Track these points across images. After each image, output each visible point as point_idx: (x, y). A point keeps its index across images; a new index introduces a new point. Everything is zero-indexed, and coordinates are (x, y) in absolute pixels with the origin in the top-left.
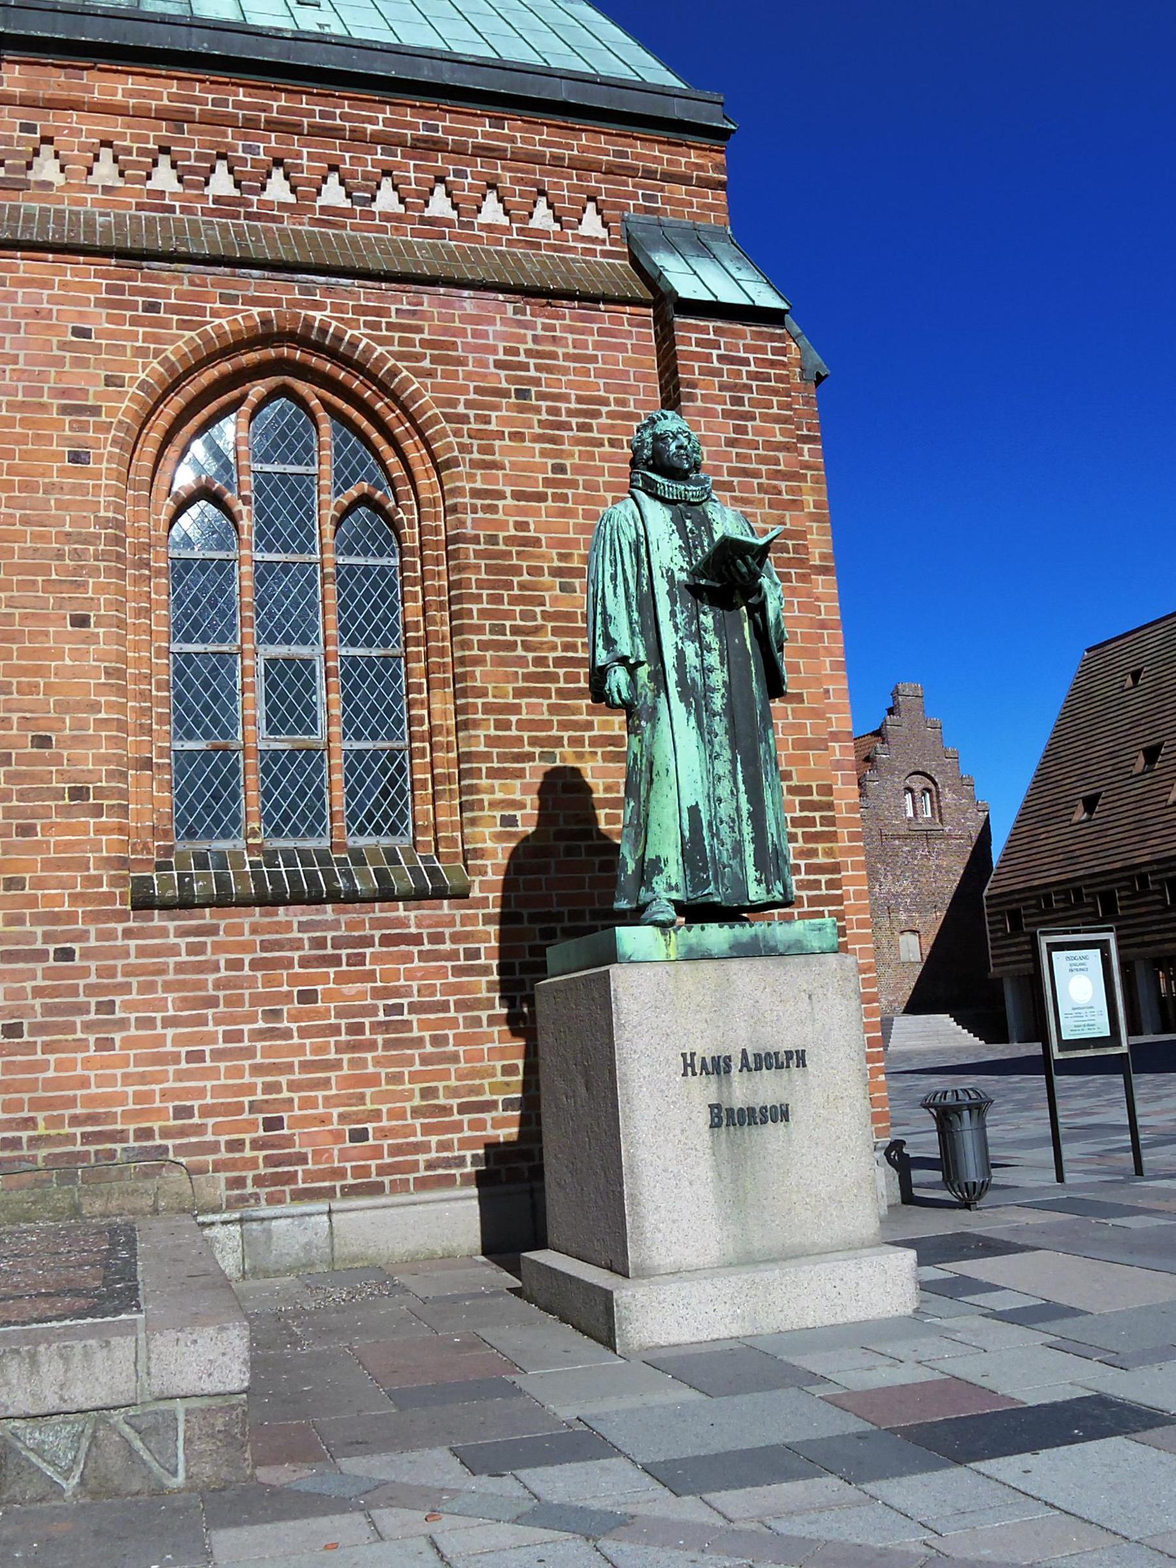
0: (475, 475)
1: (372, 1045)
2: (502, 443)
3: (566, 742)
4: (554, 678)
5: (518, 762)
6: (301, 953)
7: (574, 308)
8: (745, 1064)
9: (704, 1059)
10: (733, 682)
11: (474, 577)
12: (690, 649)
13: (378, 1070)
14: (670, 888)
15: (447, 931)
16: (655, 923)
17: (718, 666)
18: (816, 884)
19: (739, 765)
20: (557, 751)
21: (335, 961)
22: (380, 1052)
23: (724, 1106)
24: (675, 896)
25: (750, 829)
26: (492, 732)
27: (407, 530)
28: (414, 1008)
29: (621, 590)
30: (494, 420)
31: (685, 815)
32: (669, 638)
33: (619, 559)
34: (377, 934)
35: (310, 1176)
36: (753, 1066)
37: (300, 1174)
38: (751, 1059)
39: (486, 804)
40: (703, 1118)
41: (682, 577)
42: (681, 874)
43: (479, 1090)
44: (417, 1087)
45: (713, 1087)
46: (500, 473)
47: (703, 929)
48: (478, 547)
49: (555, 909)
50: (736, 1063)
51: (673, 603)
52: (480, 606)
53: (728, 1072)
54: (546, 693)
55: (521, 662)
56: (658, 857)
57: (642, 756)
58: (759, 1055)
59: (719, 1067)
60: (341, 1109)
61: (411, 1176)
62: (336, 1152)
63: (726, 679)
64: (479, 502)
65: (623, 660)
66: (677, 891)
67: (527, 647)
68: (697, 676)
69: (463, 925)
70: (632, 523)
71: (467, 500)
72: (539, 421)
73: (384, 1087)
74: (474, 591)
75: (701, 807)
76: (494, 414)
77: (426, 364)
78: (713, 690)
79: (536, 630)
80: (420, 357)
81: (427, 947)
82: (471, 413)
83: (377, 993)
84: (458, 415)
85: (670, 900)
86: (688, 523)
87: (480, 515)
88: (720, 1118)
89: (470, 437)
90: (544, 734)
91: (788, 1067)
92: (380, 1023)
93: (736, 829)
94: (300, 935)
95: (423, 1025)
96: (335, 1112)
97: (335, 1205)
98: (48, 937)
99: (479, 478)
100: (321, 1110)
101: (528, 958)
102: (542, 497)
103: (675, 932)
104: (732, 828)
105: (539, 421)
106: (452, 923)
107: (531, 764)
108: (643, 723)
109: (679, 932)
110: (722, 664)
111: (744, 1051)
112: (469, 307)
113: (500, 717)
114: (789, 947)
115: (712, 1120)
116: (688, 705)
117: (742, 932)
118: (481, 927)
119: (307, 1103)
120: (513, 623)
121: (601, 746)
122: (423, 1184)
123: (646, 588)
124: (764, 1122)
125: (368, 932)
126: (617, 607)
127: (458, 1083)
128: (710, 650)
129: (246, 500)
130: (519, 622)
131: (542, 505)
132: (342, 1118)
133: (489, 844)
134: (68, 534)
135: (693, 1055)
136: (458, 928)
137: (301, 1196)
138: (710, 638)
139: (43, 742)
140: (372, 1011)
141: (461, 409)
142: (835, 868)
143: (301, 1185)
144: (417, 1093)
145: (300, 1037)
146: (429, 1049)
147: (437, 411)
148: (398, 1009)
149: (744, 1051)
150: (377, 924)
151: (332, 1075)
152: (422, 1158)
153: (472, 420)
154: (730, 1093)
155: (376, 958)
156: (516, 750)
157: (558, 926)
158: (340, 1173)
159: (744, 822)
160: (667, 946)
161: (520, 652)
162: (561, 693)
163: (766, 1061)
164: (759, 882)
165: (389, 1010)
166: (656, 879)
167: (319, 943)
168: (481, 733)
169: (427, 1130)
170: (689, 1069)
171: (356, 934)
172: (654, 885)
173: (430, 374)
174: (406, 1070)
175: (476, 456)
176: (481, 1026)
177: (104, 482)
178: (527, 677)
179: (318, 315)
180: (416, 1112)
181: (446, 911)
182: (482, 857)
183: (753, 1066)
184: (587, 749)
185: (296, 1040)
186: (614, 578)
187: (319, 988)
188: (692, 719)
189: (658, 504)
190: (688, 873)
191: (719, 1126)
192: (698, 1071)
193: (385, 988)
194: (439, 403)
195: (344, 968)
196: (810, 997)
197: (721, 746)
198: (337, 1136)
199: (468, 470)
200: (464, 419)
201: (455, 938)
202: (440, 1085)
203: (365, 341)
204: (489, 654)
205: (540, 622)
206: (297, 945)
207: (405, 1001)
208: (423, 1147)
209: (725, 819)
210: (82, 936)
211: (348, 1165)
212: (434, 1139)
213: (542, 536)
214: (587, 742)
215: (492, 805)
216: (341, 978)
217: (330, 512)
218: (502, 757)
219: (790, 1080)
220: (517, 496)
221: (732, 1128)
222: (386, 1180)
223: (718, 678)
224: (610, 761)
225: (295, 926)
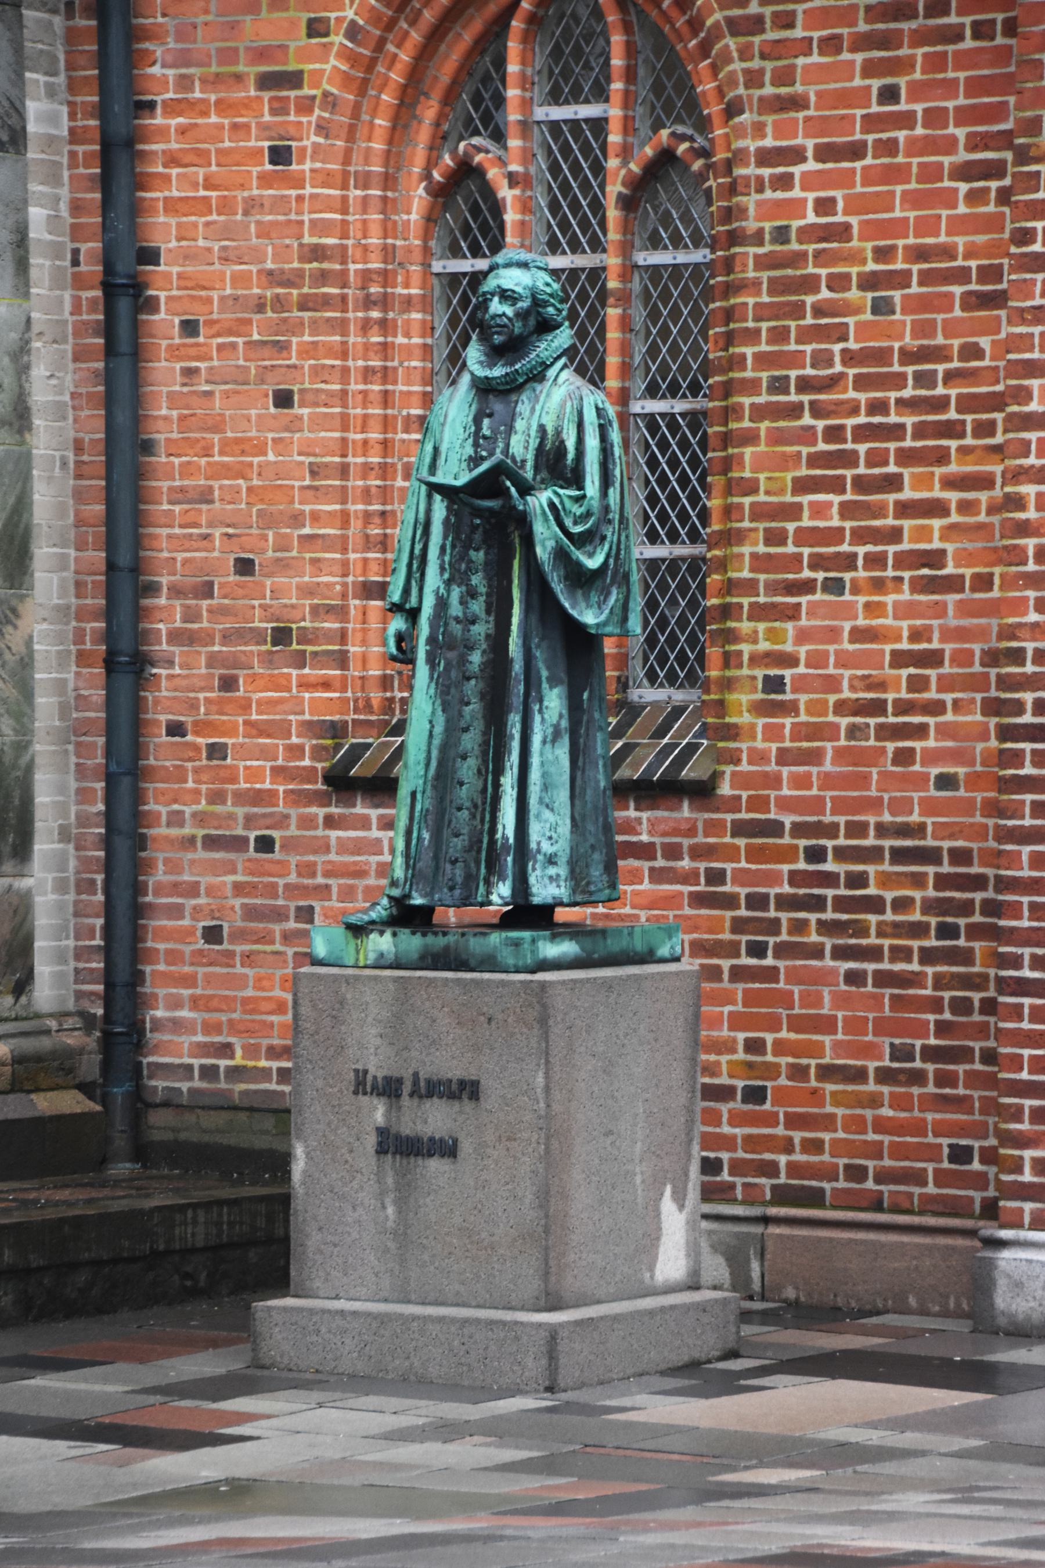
2: (809, 60)
3: (860, 562)
4: (849, 459)
5: (792, 595)
11: (751, 301)
12: (456, 592)
17: (483, 615)
20: (847, 576)
23: (393, 1131)
26: (761, 549)
32: (433, 579)
36: (423, 1091)
38: (422, 1084)
39: (746, 658)
49: (828, 819)
50: (407, 1088)
51: (445, 537)
52: (756, 349)
53: (398, 1096)
54: (836, 485)
55: (808, 435)
59: (389, 1089)
64: (766, 172)
67: (817, 410)
68: (456, 629)
69: (706, 836)
74: (750, 324)
79: (834, 382)
90: (832, 549)
98: (249, 821)
99: (769, 130)
102: (856, 151)
107: (810, 597)
110: (488, 612)
111: (416, 1075)
113: (773, 524)
118: (728, 840)
120: (801, 372)
121: (910, 569)
128: (472, 594)
129: (513, 180)
130: (809, 371)
131: (858, 165)
133: (745, 718)
134: (270, 273)
135: (366, 1072)
139: (245, 567)
149: (416, 1075)
156: (791, 576)
157: (829, 844)
161: (807, 420)
162: (861, 484)
163: (433, 1089)
168: (746, 550)
176: (721, 980)
177: (308, 190)
178: (814, 460)
182: (735, 737)
183: (423, 1091)
184: (890, 573)
191: (386, 1152)
199: (756, 118)
204: (764, 425)
205: (838, 368)
210: (282, 822)
213: (854, 221)
214: (890, 562)
217: (615, 189)
218: (773, 588)
220: (823, 153)
223: (480, 630)
224: (921, 592)
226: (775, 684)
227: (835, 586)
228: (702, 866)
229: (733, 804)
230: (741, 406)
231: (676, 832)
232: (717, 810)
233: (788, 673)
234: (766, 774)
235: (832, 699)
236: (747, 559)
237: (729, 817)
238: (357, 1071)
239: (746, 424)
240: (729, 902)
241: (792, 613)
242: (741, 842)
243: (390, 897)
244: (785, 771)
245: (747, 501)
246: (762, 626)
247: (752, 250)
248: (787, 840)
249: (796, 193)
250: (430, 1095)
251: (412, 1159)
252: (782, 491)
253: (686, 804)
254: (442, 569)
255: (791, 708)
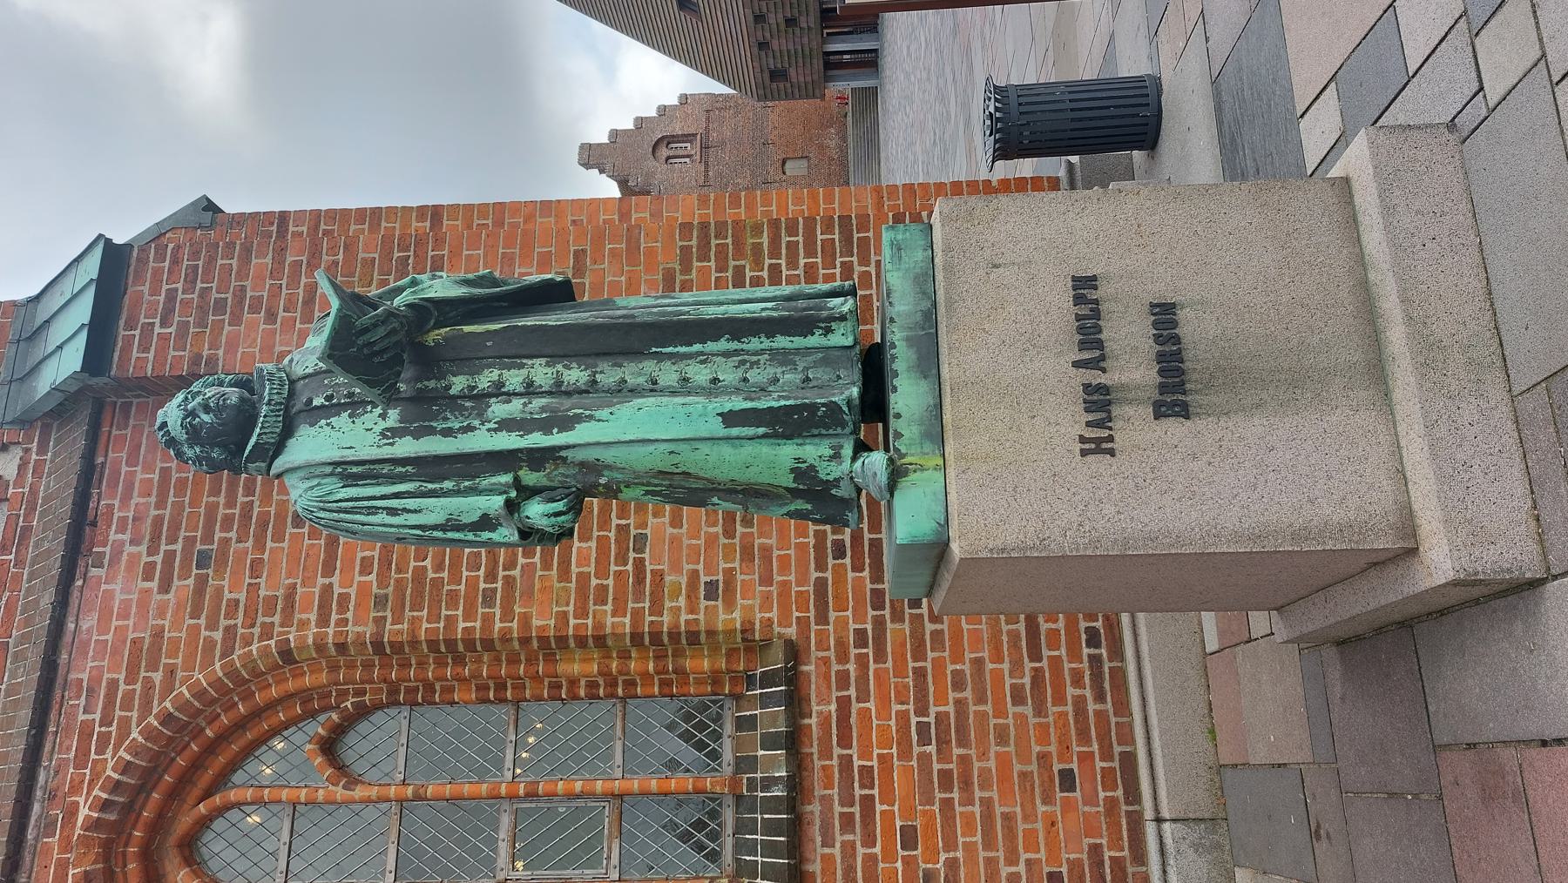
0: (300, 620)
1: (964, 761)
2: (263, 585)
6: (858, 844)
7: (99, 494)
8: (1097, 364)
9: (1088, 424)
10: (548, 351)
11: (425, 625)
12: (498, 410)
13: (992, 755)
14: (836, 456)
15: (835, 667)
16: (892, 487)
17: (524, 372)
18: (792, 247)
19: (664, 350)
20: (633, 532)
21: (868, 802)
22: (972, 752)
24: (848, 451)
25: (755, 340)
26: (609, 607)
27: (367, 698)
28: (922, 710)
29: (411, 503)
30: (233, 596)
31: (735, 431)
32: (482, 440)
33: (366, 503)
34: (837, 751)
35: (1115, 843)
36: (1097, 353)
37: (1113, 854)
38: (1086, 355)
39: (691, 617)
40: (1174, 428)
41: (394, 415)
42: (817, 440)
43: (1014, 636)
44: (1011, 709)
45: (1129, 410)
46: (299, 590)
47: (898, 416)
48: (389, 620)
49: (812, 541)
51: (431, 431)
53: (1103, 389)
56: (793, 470)
57: (648, 484)
58: (1081, 342)
59: (1099, 402)
60: (1038, 801)
61: (1113, 720)
62: (1086, 809)
63: (543, 361)
64: (334, 617)
65: (511, 507)
66: (841, 447)
68: (538, 403)
70: (315, 482)
71: (330, 631)
72: (239, 541)
73: (1011, 749)
74: (442, 625)
75: (728, 407)
76: (227, 595)
77: (157, 677)
78: (559, 383)
80: (148, 685)
81: (852, 692)
82: (223, 623)
83: (905, 754)
84: (224, 639)
85: (854, 459)
86: (317, 402)
87: (350, 615)
88: (1175, 404)
89: (253, 625)
91: (1096, 302)
92: (939, 751)
93: (755, 358)
94: (838, 845)
95: (941, 699)
96: (1041, 808)
97: (1149, 814)
99: (304, 616)
100: (1039, 826)
101: (866, 573)
103: (903, 456)
104: (753, 364)
105: (239, 541)
106: (826, 661)
108: (603, 481)
109: (903, 451)
110: (522, 366)
111: (1076, 364)
112: (89, 622)
114: (924, 293)
115: (1177, 415)
116: (578, 419)
117: (902, 359)
118: (831, 628)
119: (1031, 845)
122: (1122, 706)
123: (409, 468)
124: (1176, 340)
125: (835, 762)
126: (436, 510)
127: (1007, 659)
130: (482, 572)
132: (1048, 800)
133: (737, 615)
135: (1083, 440)
136: (832, 654)
137: (1139, 856)
138: (485, 380)
140: (924, 759)
141: (218, 636)
142: (774, 225)
143: (1126, 853)
144: (1019, 709)
145: (956, 849)
146: (968, 694)
147: (218, 665)
148: (923, 729)
149: (1076, 364)
150: (826, 753)
151: (998, 810)
152: (1092, 707)
153: (232, 622)
154: (1138, 387)
155: (865, 754)
158: (1111, 804)
159: (744, 346)
160: (922, 468)
161: (516, 572)
164: (828, 331)
165: (924, 740)
166: (822, 476)
167: (847, 821)
168: (609, 620)
169: (1060, 699)
170: (1104, 446)
171: (837, 775)
172: (830, 478)
173: (171, 672)
174: (993, 722)
175: (277, 619)
179: (83, 812)
180: (1040, 711)
181: (812, 667)
183: (1097, 353)
185: (959, 854)
186: (393, 512)
187: (898, 824)
188: (598, 414)
189: (291, 442)
190: (816, 432)
192: (1105, 433)
193: (899, 744)
194: (208, 662)
195: (876, 792)
196: (996, 266)
197: (640, 375)
198: (1067, 806)
199: (294, 629)
200: (230, 631)
201: (843, 657)
202: (1008, 682)
203: (122, 753)
206: (849, 850)
207: (914, 720)
208: (1080, 703)
209: (740, 373)
211: (1102, 795)
212: (1071, 691)
215: (692, 610)
216: (887, 798)
217: (340, 792)
218: (639, 597)
219: (1116, 300)
220: (329, 570)
221: (1188, 386)
222: (1117, 749)
223: (541, 372)
225: (827, 850)
226: (711, 591)
227: (641, 541)
228: (853, 651)
229: (803, 623)
230: (501, 629)
231: (827, 677)
232: (809, 638)
233: (704, 579)
234: (779, 595)
235: (723, 540)
236: (616, 619)
237: (814, 627)
238: (1084, 453)
239: (515, 625)
240: (879, 623)
241: (659, 576)
242: (832, 615)
243: (854, 459)
244: (777, 578)
245: (572, 622)
246: (668, 604)
247: (388, 627)
248: (829, 575)
249: (353, 591)
250: (1099, 344)
251: (1187, 365)
252: (567, 590)
253: (805, 668)
254: (469, 429)
255: (729, 573)
